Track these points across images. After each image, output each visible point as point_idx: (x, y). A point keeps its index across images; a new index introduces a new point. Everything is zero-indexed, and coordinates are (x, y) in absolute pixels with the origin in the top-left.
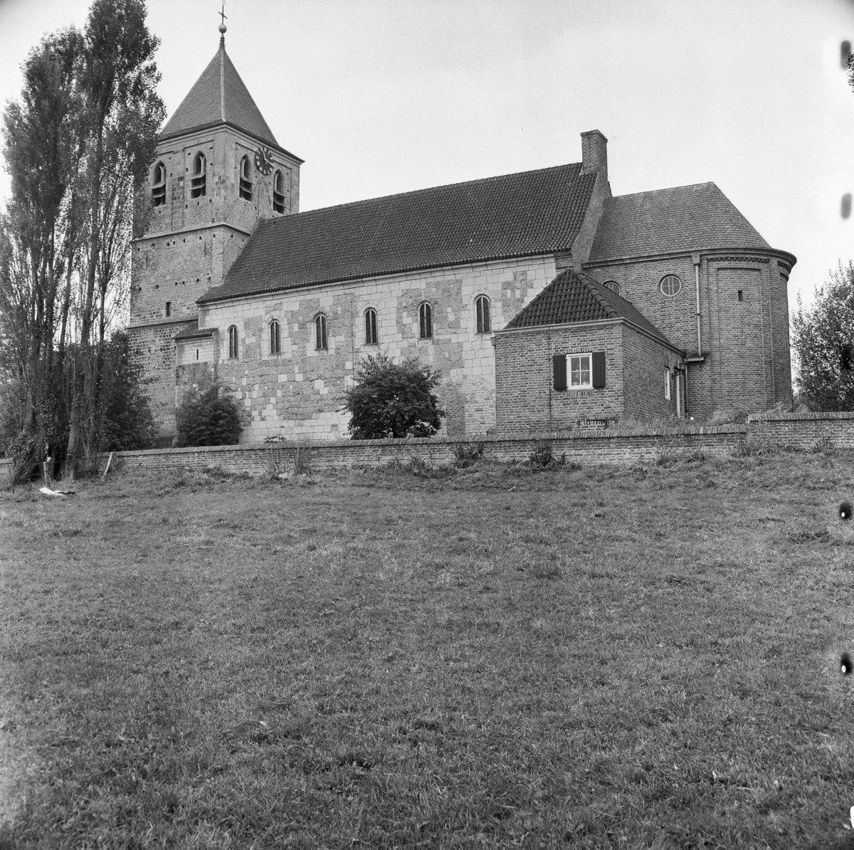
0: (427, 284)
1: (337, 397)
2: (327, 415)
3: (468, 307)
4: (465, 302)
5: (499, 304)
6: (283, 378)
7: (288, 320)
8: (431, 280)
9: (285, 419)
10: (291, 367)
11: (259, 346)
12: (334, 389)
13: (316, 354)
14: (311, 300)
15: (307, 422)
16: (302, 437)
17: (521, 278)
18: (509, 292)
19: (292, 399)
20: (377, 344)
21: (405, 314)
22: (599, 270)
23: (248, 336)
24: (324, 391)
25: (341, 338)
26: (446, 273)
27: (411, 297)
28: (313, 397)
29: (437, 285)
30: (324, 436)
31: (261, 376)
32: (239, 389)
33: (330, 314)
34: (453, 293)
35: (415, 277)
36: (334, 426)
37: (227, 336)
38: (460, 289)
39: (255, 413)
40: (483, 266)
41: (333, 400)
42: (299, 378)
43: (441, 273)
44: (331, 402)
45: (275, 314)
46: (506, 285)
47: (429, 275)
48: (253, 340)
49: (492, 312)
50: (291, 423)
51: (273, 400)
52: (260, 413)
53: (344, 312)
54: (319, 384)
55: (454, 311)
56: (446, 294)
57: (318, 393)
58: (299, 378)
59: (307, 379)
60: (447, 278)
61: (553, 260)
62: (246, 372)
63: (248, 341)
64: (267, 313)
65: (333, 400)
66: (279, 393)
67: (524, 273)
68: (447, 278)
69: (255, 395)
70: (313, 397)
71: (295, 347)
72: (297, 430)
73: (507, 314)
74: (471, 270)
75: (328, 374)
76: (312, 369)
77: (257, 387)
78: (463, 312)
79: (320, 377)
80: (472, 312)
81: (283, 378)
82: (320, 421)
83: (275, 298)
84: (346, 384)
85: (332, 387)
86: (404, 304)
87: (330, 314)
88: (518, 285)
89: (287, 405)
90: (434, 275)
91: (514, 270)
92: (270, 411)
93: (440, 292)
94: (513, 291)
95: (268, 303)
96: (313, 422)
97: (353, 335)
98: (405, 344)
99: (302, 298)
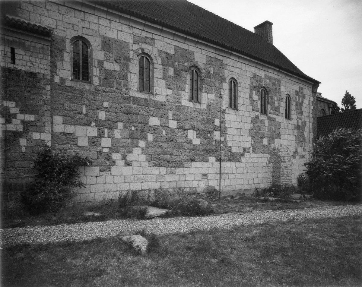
1: (207, 148)
2: (199, 164)
6: (154, 121)
7: (163, 61)
9: (156, 165)
10: (165, 112)
11: (125, 77)
12: (205, 141)
13: (191, 105)
14: (186, 50)
15: (179, 170)
16: (173, 185)
19: (165, 145)
20: (237, 110)
21: (254, 92)
23: (108, 60)
24: (197, 142)
25: (212, 96)
28: (186, 146)
29: (270, 78)
30: (195, 184)
31: (127, 114)
32: (93, 124)
33: (204, 71)
36: (205, 175)
37: (69, 47)
39: (116, 156)
41: (203, 150)
42: (173, 124)
44: (202, 153)
45: (148, 48)
48: (117, 67)
50: (163, 170)
51: (142, 144)
52: (124, 158)
53: (216, 74)
54: (192, 134)
57: (190, 142)
58: (173, 124)
59: (181, 128)
62: (106, 104)
63: (108, 66)
64: (135, 42)
65: (203, 150)
66: (150, 137)
69: (117, 134)
70: (186, 146)
71: (169, 92)
72: (169, 178)
75: (200, 126)
76: (186, 118)
77: (120, 125)
79: (193, 128)
81: (154, 121)
82: (192, 170)
83: (146, 29)
84: (215, 138)
85: (204, 139)
87: (204, 71)
89: (159, 150)
92: (137, 155)
95: (137, 32)
96: (185, 170)
97: (221, 97)
98: (253, 114)
99: (176, 43)
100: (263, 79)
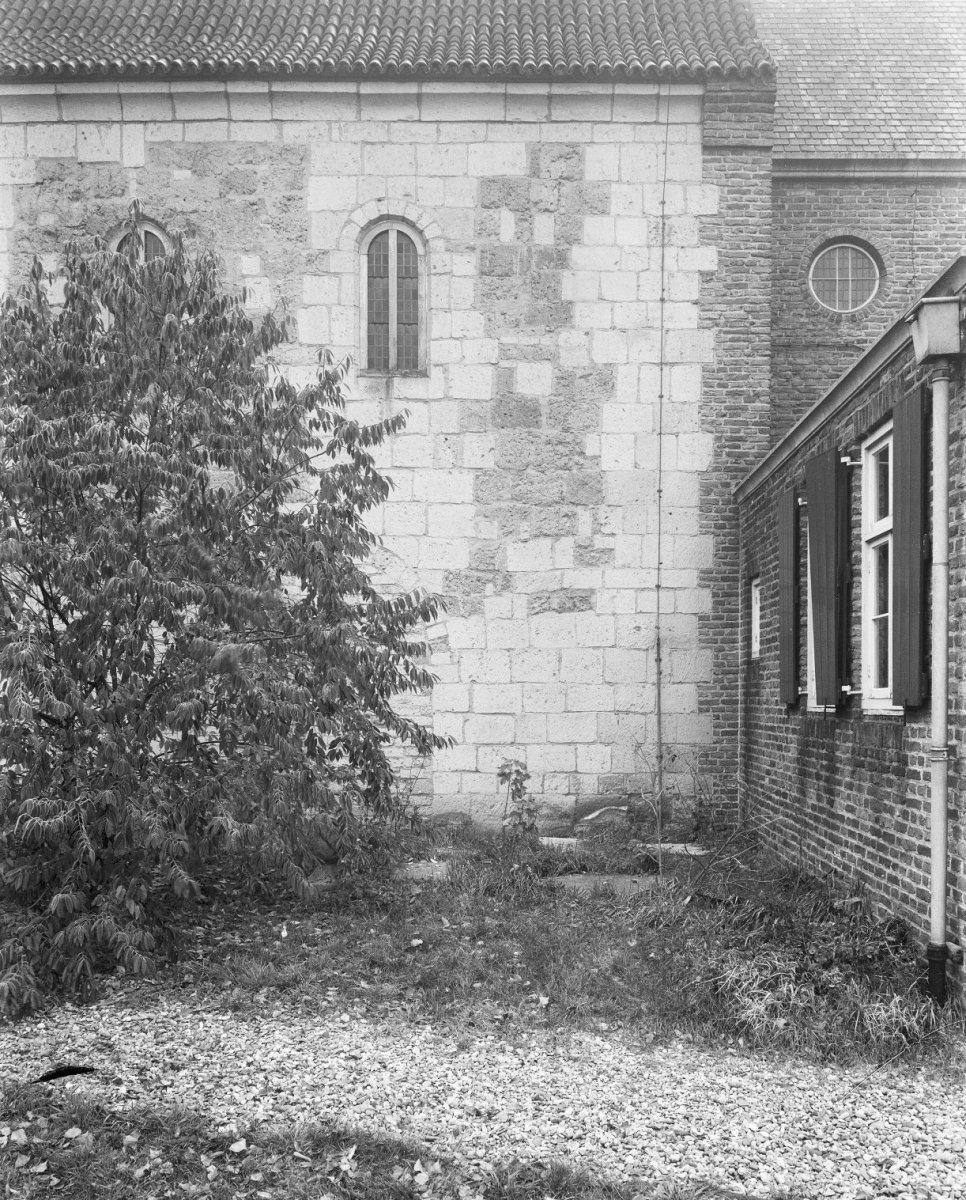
0: (152, 148)
3: (334, 263)
4: (317, 242)
5: (466, 265)
8: (173, 132)
17: (559, 168)
18: (507, 224)
22: (807, 193)
26: (239, 111)
27: (77, 196)
34: (271, 197)
35: (100, 112)
38: (296, 184)
40: (404, 99)
43: (217, 110)
46: (498, 192)
47: (161, 112)
49: (433, 291)
55: (268, 270)
56: (238, 200)
60: (245, 134)
61: (691, 113)
67: (572, 152)
68: (245, 134)
73: (501, 305)
74: (349, 114)
78: (307, 279)
80: (348, 282)
86: (47, 221)
88: (544, 193)
90: (183, 112)
91: (532, 134)
93: (211, 186)
94: (524, 213)
100: (133, 174)
